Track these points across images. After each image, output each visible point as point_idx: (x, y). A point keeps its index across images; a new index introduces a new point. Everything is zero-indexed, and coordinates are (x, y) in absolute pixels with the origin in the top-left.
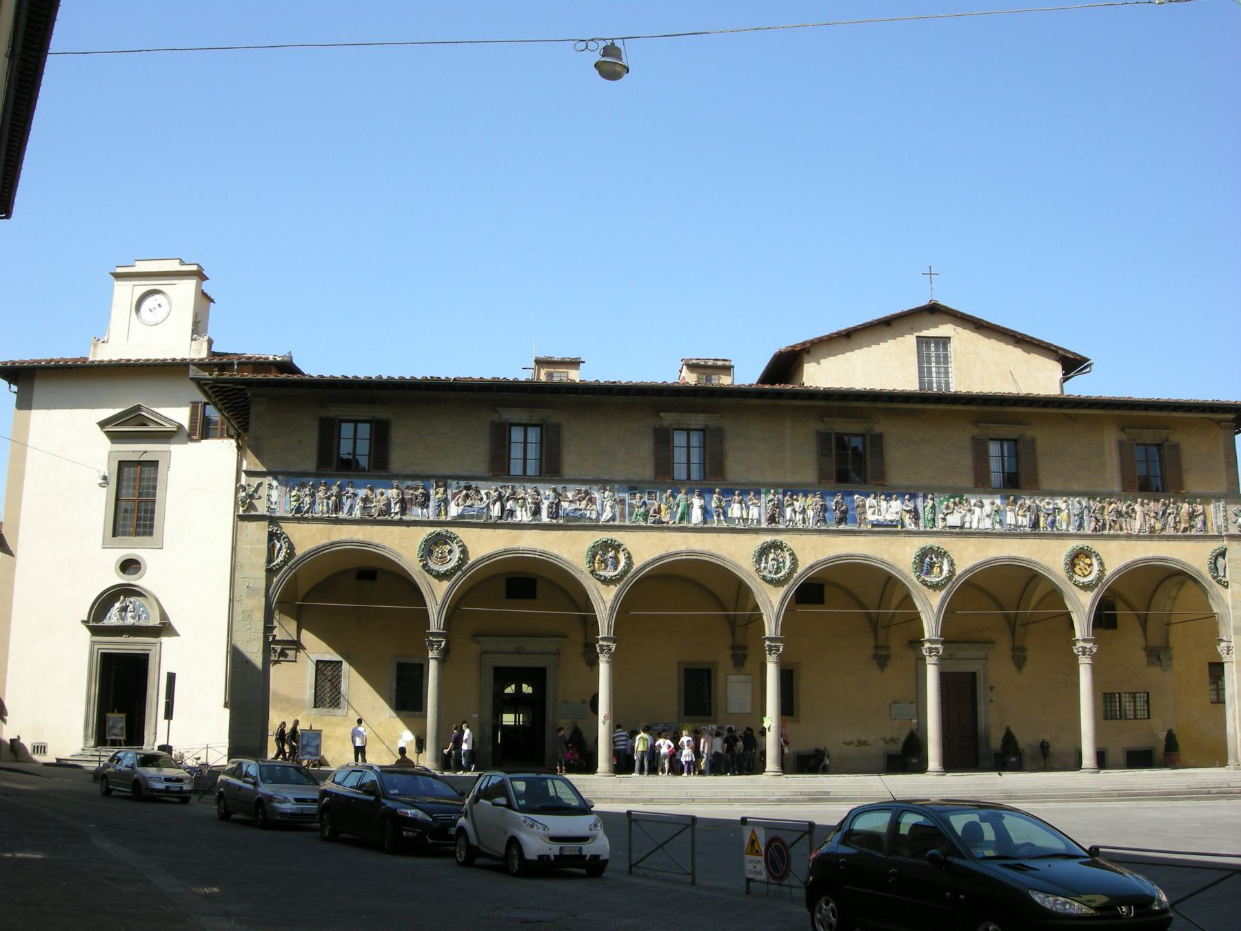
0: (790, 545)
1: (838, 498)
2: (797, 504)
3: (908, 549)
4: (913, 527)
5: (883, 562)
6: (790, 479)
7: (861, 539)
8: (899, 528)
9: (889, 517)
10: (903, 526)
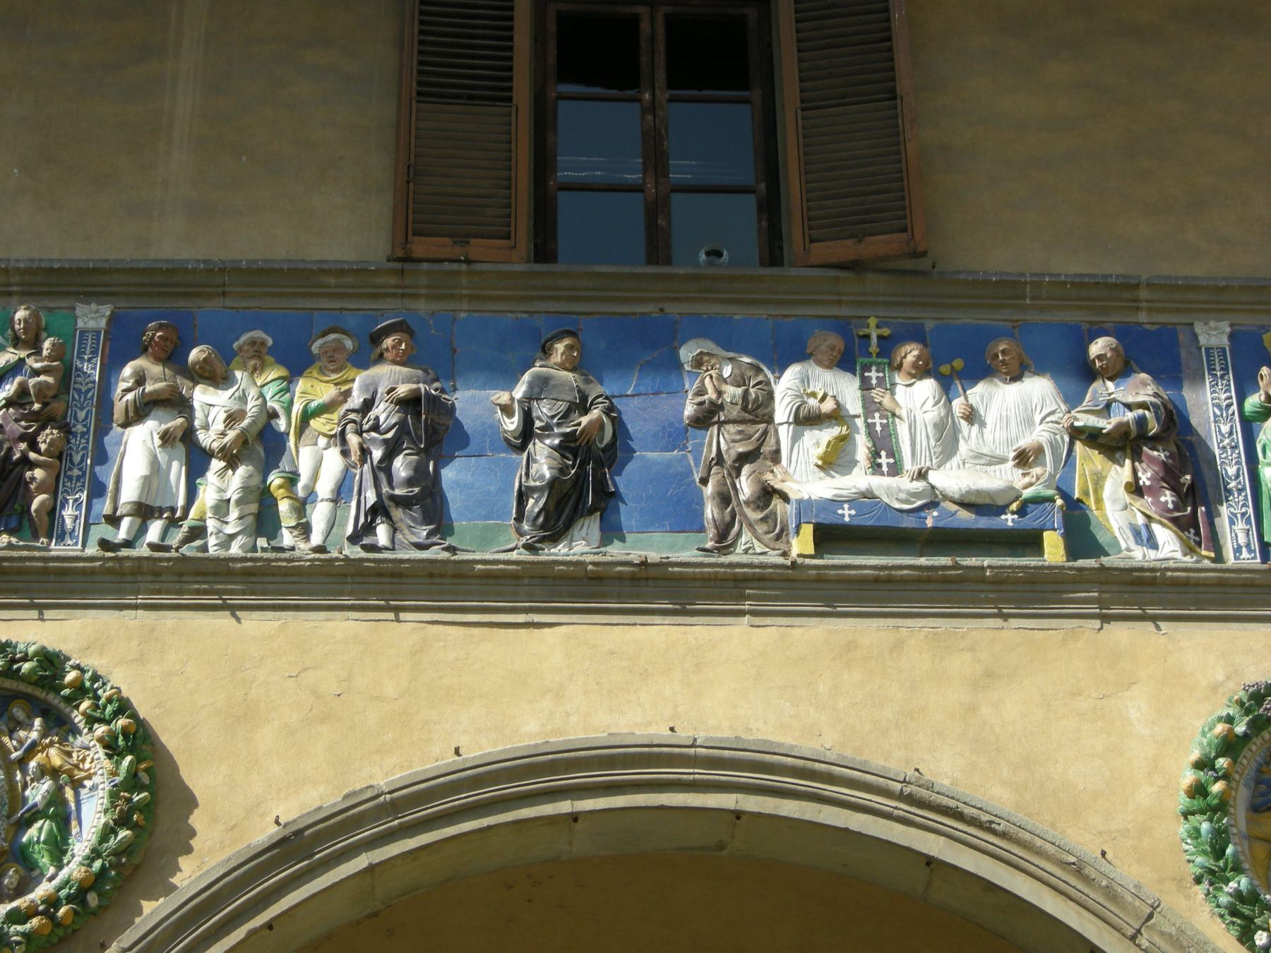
0: (121, 679)
1: (556, 365)
2: (211, 404)
3: (1136, 707)
4: (1168, 546)
7: (734, 640)
8: (1054, 549)
10: (1081, 534)
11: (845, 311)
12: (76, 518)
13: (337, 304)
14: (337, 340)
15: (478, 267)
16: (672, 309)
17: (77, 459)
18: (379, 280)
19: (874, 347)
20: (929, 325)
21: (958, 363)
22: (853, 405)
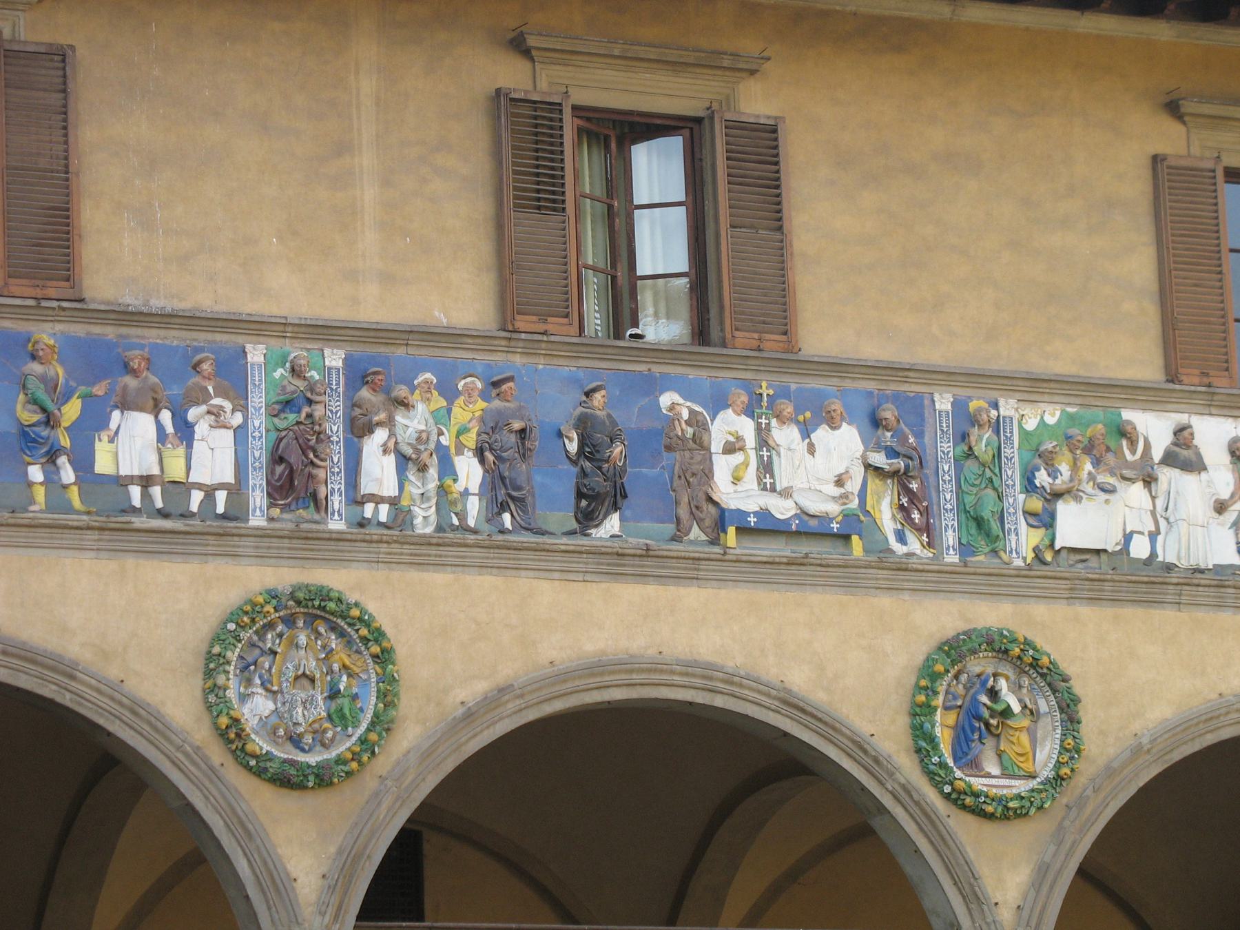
5: (793, 704)
6: (374, 307)
9: (823, 503)
11: (749, 375)
12: (340, 502)
13: (470, 355)
14: (473, 382)
15: (552, 338)
16: (656, 369)
17: (336, 460)
18: (496, 342)
19: (765, 404)
20: (793, 387)
21: (808, 414)
22: (751, 441)
